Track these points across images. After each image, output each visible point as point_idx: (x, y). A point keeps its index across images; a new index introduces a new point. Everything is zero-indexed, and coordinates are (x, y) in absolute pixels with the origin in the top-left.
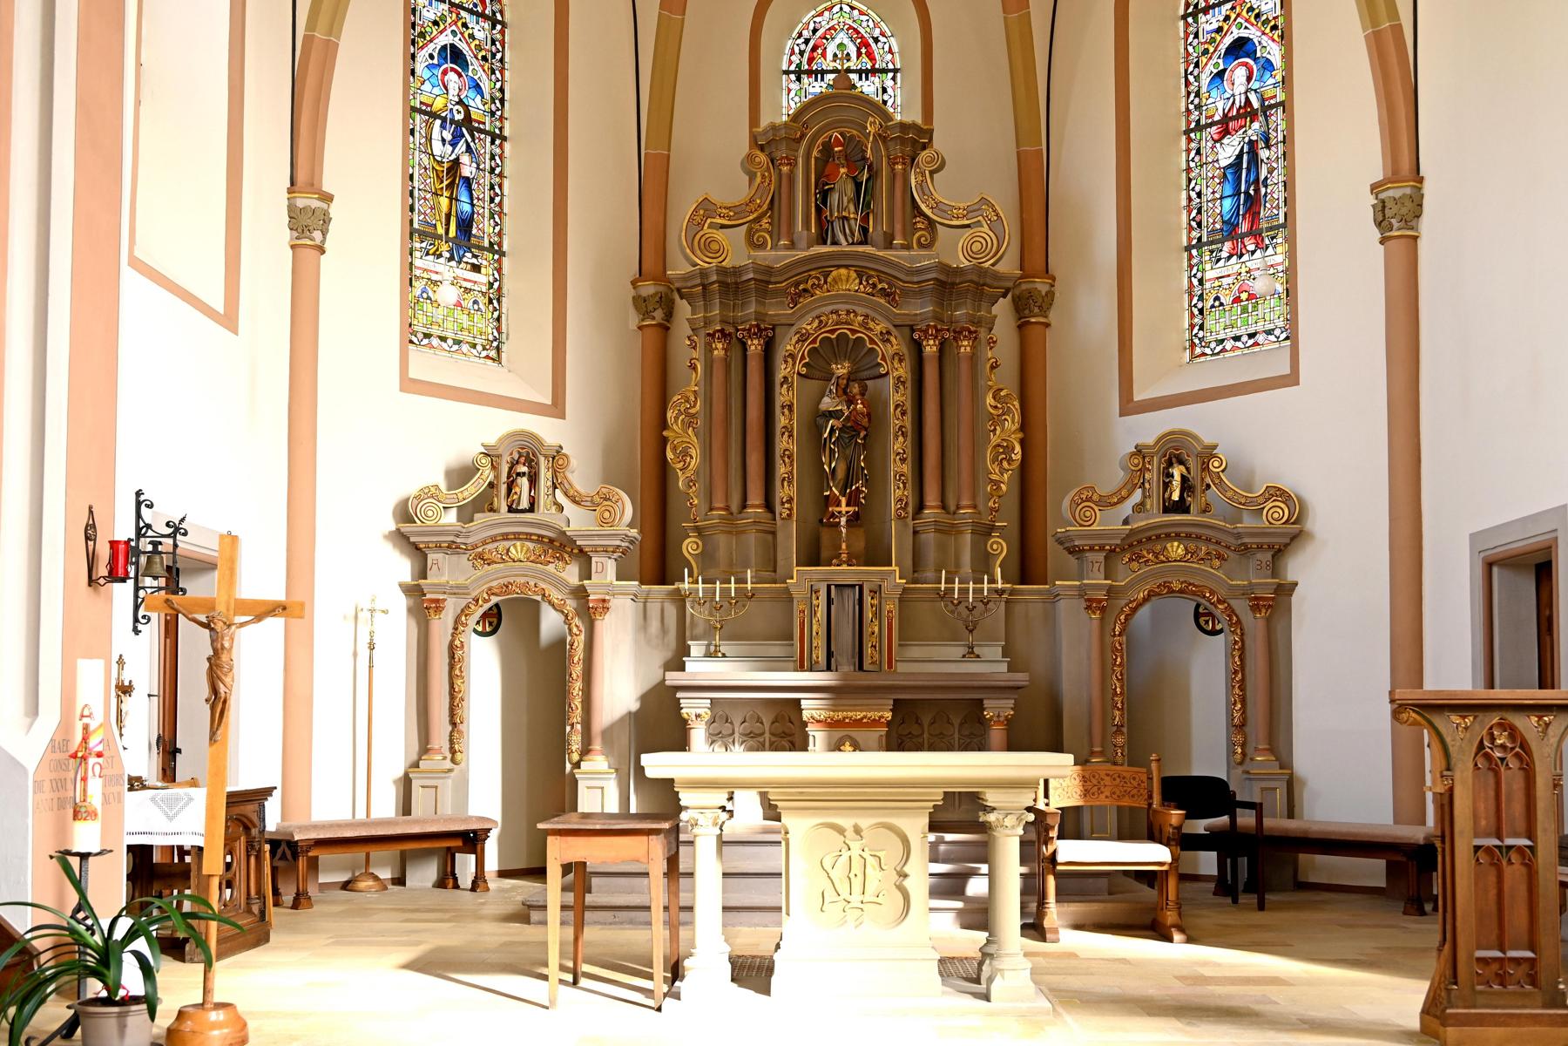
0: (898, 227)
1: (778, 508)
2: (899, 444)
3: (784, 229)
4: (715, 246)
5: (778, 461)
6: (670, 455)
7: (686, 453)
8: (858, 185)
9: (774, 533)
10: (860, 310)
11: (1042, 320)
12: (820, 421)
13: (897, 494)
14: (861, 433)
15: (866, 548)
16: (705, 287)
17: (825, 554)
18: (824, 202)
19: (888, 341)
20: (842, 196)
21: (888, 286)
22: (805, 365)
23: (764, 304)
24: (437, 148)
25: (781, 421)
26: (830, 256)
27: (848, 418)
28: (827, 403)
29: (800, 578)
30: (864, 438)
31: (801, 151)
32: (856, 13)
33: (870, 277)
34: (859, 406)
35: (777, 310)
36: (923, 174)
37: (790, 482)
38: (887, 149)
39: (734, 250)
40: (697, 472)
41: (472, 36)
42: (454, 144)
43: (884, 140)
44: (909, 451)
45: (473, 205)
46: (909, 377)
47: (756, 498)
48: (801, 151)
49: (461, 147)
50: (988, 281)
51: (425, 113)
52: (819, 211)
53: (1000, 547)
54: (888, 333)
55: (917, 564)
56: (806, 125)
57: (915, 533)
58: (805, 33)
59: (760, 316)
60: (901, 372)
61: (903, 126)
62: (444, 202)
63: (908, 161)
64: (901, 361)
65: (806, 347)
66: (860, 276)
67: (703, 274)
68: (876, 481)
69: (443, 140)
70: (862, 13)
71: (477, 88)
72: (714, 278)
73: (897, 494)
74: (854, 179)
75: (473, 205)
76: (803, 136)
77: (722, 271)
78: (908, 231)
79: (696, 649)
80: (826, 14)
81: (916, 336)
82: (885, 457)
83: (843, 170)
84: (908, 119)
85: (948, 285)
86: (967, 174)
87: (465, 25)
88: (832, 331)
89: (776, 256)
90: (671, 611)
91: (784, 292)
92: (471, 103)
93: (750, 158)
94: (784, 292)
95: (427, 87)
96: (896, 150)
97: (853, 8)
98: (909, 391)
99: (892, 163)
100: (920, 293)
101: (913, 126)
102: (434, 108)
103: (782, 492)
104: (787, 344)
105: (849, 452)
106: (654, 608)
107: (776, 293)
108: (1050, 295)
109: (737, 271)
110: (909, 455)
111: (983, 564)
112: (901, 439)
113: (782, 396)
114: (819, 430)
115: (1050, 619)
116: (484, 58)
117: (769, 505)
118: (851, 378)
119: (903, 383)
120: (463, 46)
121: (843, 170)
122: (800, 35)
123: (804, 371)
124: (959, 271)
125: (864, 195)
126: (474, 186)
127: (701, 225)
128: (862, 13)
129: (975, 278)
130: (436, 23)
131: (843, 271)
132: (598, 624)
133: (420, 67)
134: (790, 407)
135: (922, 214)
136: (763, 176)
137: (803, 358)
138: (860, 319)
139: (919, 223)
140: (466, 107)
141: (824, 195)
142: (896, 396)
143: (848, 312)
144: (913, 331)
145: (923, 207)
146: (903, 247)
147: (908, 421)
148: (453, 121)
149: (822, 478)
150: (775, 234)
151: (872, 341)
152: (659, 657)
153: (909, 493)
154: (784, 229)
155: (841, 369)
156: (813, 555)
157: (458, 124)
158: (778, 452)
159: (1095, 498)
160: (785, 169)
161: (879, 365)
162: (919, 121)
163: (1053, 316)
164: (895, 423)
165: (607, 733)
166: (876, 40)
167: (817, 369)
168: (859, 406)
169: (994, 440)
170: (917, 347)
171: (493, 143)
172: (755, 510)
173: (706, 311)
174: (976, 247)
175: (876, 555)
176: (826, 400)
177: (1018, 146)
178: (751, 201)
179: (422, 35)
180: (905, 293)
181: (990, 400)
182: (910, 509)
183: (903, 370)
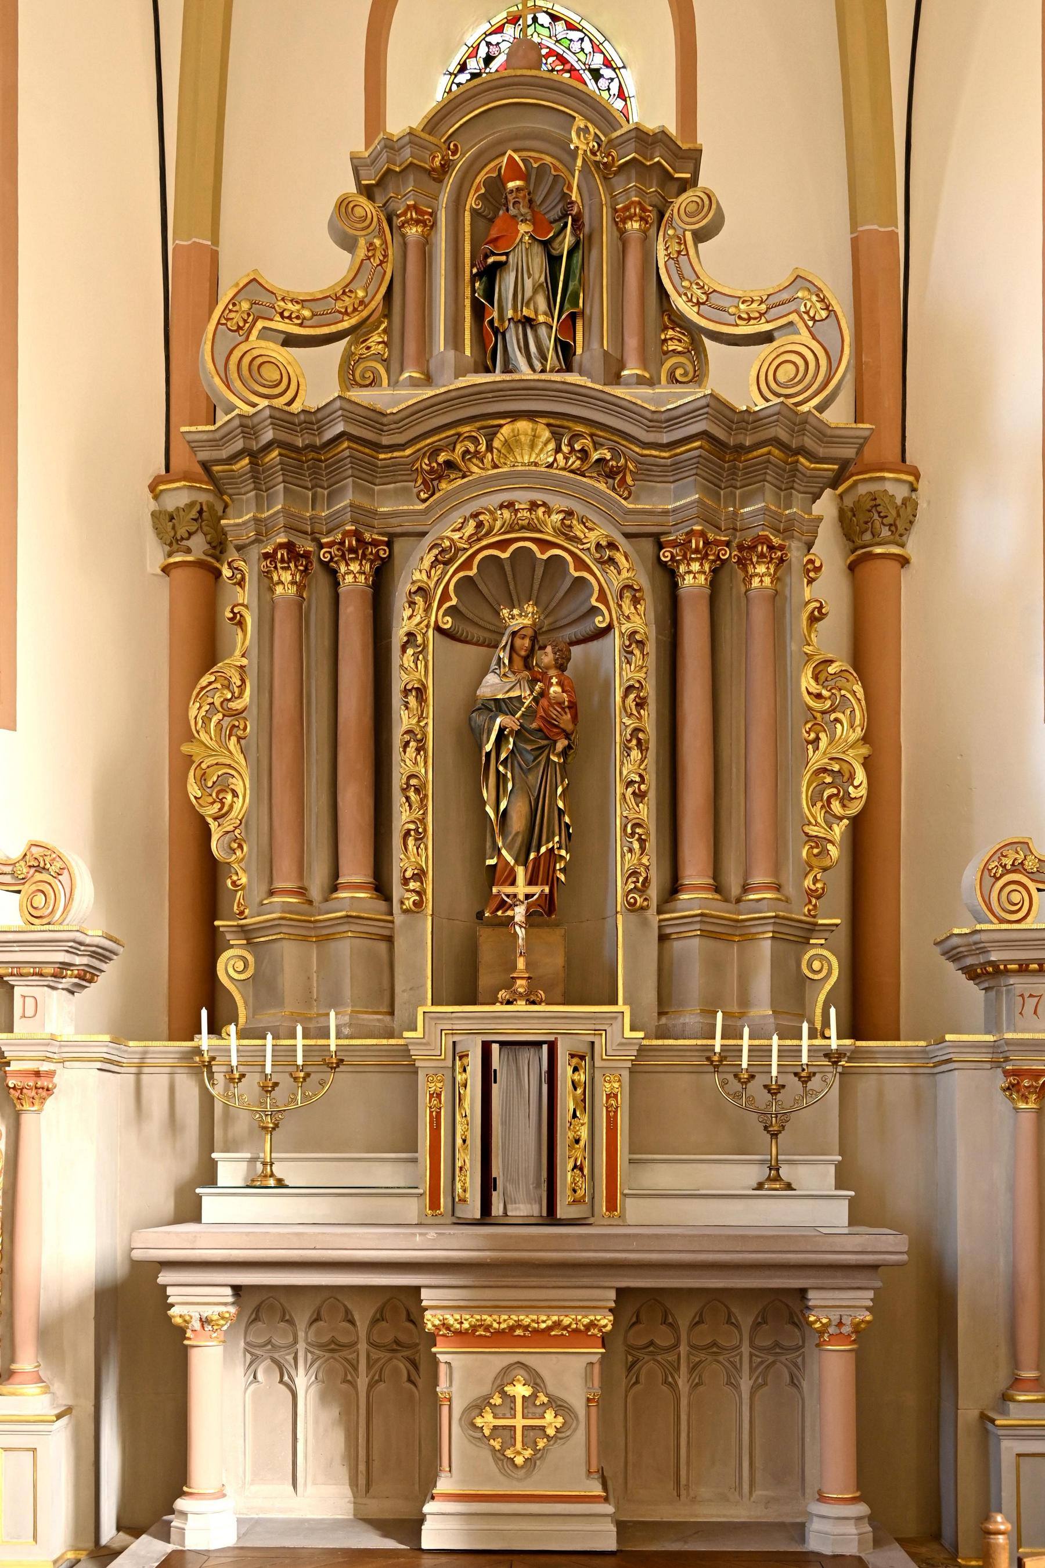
0: (632, 343)
1: (397, 891)
2: (631, 766)
3: (411, 348)
4: (270, 374)
5: (398, 798)
6: (194, 790)
7: (224, 787)
8: (553, 261)
9: (389, 940)
10: (558, 502)
11: (895, 550)
12: (479, 719)
13: (628, 862)
14: (556, 740)
15: (569, 965)
16: (255, 456)
17: (485, 980)
18: (489, 295)
19: (611, 560)
20: (523, 277)
21: (609, 450)
22: (452, 611)
23: (371, 494)
25: (403, 719)
26: (496, 392)
27: (531, 713)
28: (493, 686)
29: (435, 1029)
30: (565, 753)
31: (444, 198)
32: (560, 26)
33: (576, 436)
34: (555, 689)
35: (394, 504)
36: (682, 241)
37: (420, 839)
38: (610, 189)
39: (316, 379)
40: (244, 822)
43: (607, 172)
44: (651, 778)
46: (653, 636)
47: (355, 870)
48: (444, 198)
50: (808, 442)
52: (478, 310)
53: (825, 966)
54: (612, 545)
55: (665, 1002)
56: (452, 146)
57: (663, 938)
58: (473, 65)
59: (362, 515)
60: (637, 623)
61: (642, 138)
63: (652, 216)
64: (636, 601)
65: (452, 576)
66: (557, 437)
67: (247, 427)
68: (586, 833)
70: (570, 27)
72: (268, 435)
73: (628, 862)
74: (546, 245)
76: (446, 167)
77: (282, 419)
78: (653, 354)
79: (231, 1170)
80: (509, 29)
81: (665, 556)
82: (606, 790)
83: (523, 228)
84: (651, 125)
85: (729, 449)
86: (764, 228)
88: (502, 545)
89: (393, 396)
90: (188, 1089)
91: (410, 470)
93: (344, 206)
94: (410, 470)
96: (628, 188)
97: (555, 18)
98: (651, 661)
99: (620, 219)
100: (673, 471)
101: (661, 138)
103: (405, 859)
104: (416, 569)
105: (534, 779)
106: (156, 1085)
107: (392, 472)
108: (910, 505)
109: (313, 420)
110: (651, 785)
111: (792, 993)
112: (635, 754)
113: (405, 670)
114: (476, 737)
115: (925, 1108)
118: (537, 639)
119: (641, 644)
121: (523, 228)
122: (463, 68)
123: (447, 623)
124: (749, 420)
125: (564, 277)
127: (243, 330)
128: (570, 27)
129: (783, 435)
131: (523, 425)
132: (27, 1119)
134: (420, 692)
135: (678, 321)
136: (371, 246)
137: (445, 597)
138: (556, 518)
139: (677, 335)
141: (489, 274)
142: (625, 669)
143: (534, 506)
144: (660, 546)
145: (679, 303)
146: (640, 381)
147: (649, 719)
149: (482, 831)
150: (393, 363)
151: (581, 564)
152: (161, 1176)
153: (650, 861)
154: (411, 348)
155: (520, 618)
156: (463, 984)
159: (1030, 864)
160: (413, 232)
161: (594, 611)
162: (672, 129)
163: (913, 548)
164: (623, 724)
165: (48, 1336)
166: (596, 74)
167: (470, 623)
168: (555, 689)
169: (816, 759)
170: (669, 576)
172: (356, 896)
173: (259, 508)
174: (786, 373)
175: (585, 982)
176: (491, 679)
177: (854, 223)
178: (346, 290)
180: (646, 471)
181: (807, 682)
182: (653, 892)
183: (639, 620)
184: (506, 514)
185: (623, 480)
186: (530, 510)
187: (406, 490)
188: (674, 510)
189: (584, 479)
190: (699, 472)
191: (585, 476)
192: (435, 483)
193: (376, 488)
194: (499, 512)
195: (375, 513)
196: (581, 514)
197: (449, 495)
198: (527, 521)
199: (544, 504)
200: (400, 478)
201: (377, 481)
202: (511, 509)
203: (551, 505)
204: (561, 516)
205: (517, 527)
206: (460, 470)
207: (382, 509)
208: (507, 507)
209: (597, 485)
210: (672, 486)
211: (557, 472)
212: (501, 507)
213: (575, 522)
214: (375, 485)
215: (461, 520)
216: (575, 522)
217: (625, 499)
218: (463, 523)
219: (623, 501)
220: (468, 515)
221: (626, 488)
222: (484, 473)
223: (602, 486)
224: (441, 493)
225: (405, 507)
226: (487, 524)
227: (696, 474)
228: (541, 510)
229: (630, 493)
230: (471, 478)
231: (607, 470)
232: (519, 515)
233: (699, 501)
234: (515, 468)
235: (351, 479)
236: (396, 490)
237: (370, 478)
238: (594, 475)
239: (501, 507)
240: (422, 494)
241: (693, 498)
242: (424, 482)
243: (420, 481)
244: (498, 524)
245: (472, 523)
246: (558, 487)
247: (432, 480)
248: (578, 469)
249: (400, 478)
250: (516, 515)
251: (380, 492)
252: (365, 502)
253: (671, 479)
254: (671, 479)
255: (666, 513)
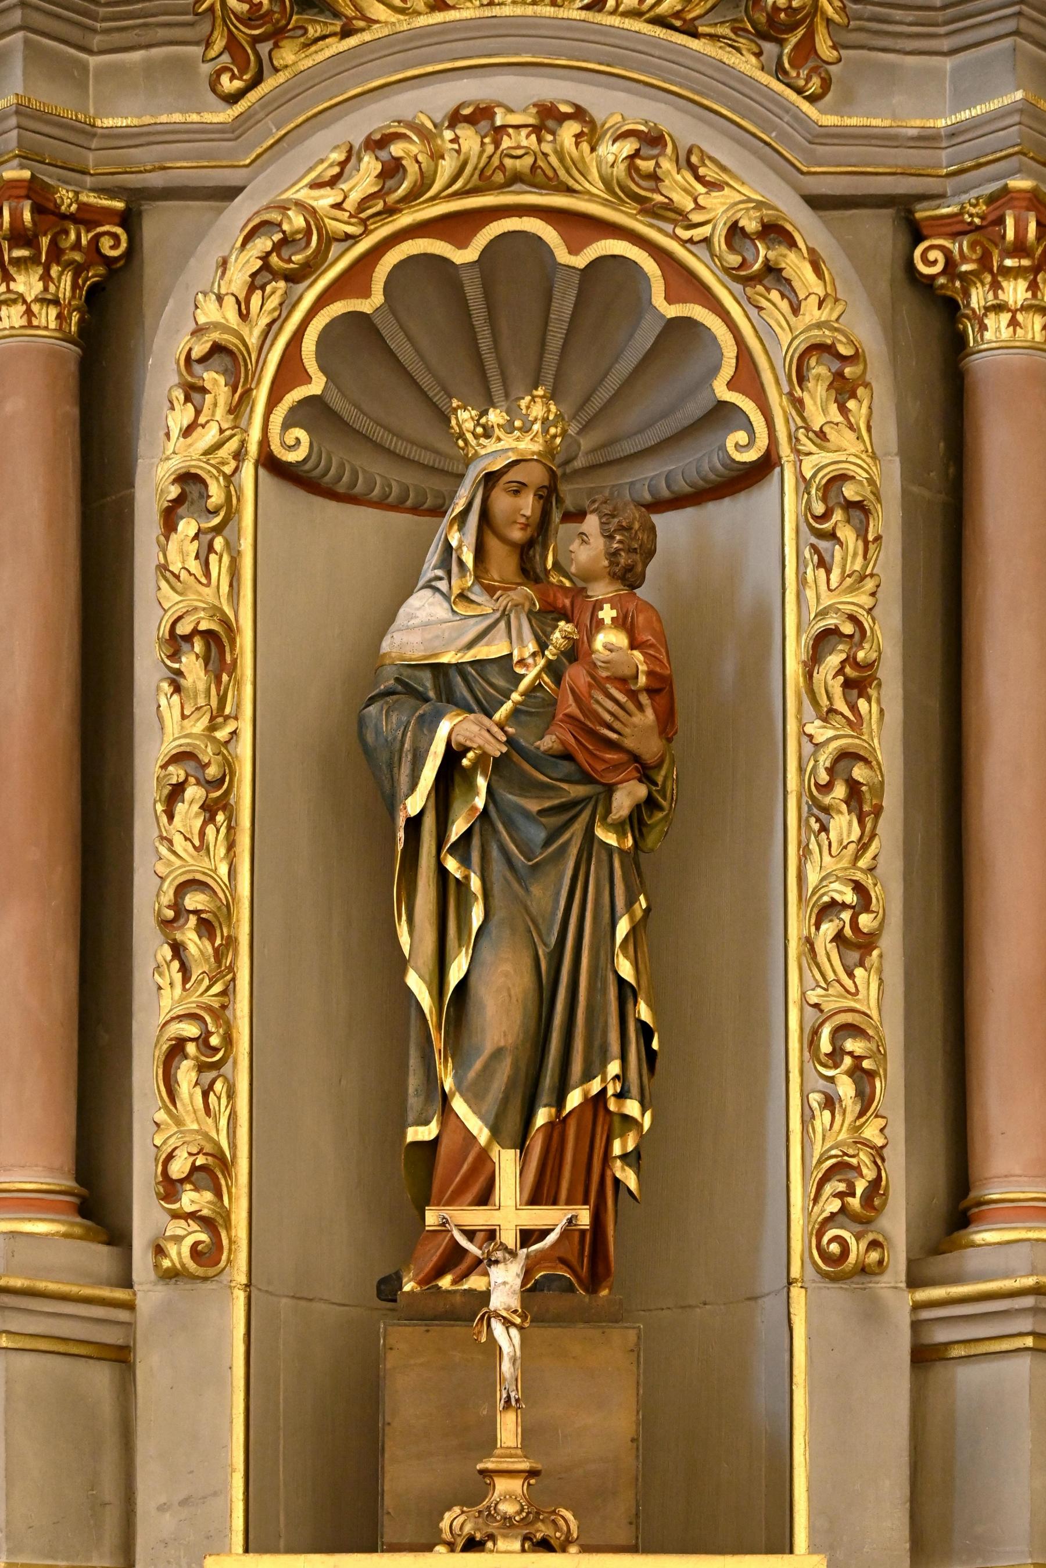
1: (146, 1216)
2: (830, 865)
5: (149, 949)
9: (121, 1357)
10: (613, 107)
12: (388, 722)
13: (821, 1130)
14: (612, 788)
15: (647, 1439)
17: (403, 1477)
19: (772, 272)
22: (313, 413)
23: (76, 77)
25: (165, 722)
27: (538, 707)
28: (429, 626)
30: (637, 821)
34: (608, 641)
37: (213, 1064)
44: (889, 893)
46: (892, 484)
54: (774, 231)
57: (925, 1356)
60: (846, 451)
64: (843, 389)
65: (311, 313)
73: (821, 1130)
81: (929, 261)
82: (757, 926)
88: (456, 226)
98: (889, 561)
103: (165, 1125)
104: (205, 292)
105: (547, 895)
110: (889, 915)
112: (844, 825)
113: (171, 580)
114: (377, 773)
117: (96, 1200)
118: (556, 498)
123: (296, 446)
134: (216, 644)
137: (291, 370)
138: (614, 152)
142: (806, 577)
143: (548, 117)
144: (916, 234)
147: (884, 727)
149: (397, 1044)
151: (684, 282)
153: (890, 1134)
155: (509, 435)
158: (149, 894)
161: (722, 415)
164: (807, 737)
168: (608, 641)
176: (424, 608)
182: (896, 1224)
183: (856, 442)
184: (470, 139)
185: (807, 48)
186: (537, 130)
187: (183, 68)
188: (953, 133)
189: (695, 44)
190: (1025, 26)
191: (695, 35)
192: (264, 48)
193: (93, 61)
194: (448, 135)
195: (89, 131)
196: (686, 140)
197: (304, 84)
198: (529, 160)
199: (579, 113)
200: (162, 33)
201: (96, 41)
202: (484, 125)
203: (598, 116)
204: (628, 147)
205: (499, 177)
206: (337, 15)
207: (109, 122)
208: (471, 120)
209: (731, 58)
210: (948, 63)
211: (616, 21)
212: (455, 119)
213: (667, 165)
214: (90, 52)
215: (338, 156)
216: (667, 165)
217: (812, 99)
218: (343, 164)
219: (805, 106)
220: (358, 141)
221: (814, 70)
222: (404, 23)
223: (746, 64)
224: (281, 77)
225: (177, 117)
226: (412, 169)
227: (1016, 33)
228: (569, 130)
229: (826, 84)
230: (366, 36)
231: (762, 18)
232: (506, 143)
233: (1027, 109)
234: (496, 11)
235: (20, 35)
236: (149, 68)
237: (75, 34)
238: (724, 30)
239: (455, 119)
240: (225, 79)
241: (1007, 100)
242: (232, 45)
243: (219, 44)
244: (447, 167)
245: (370, 165)
246: (615, 64)
247: (255, 40)
248: (677, 15)
249: (162, 33)
250: (497, 144)
251: (103, 72)
252: (56, 99)
253: (946, 44)
254: (946, 44)
255: (928, 139)
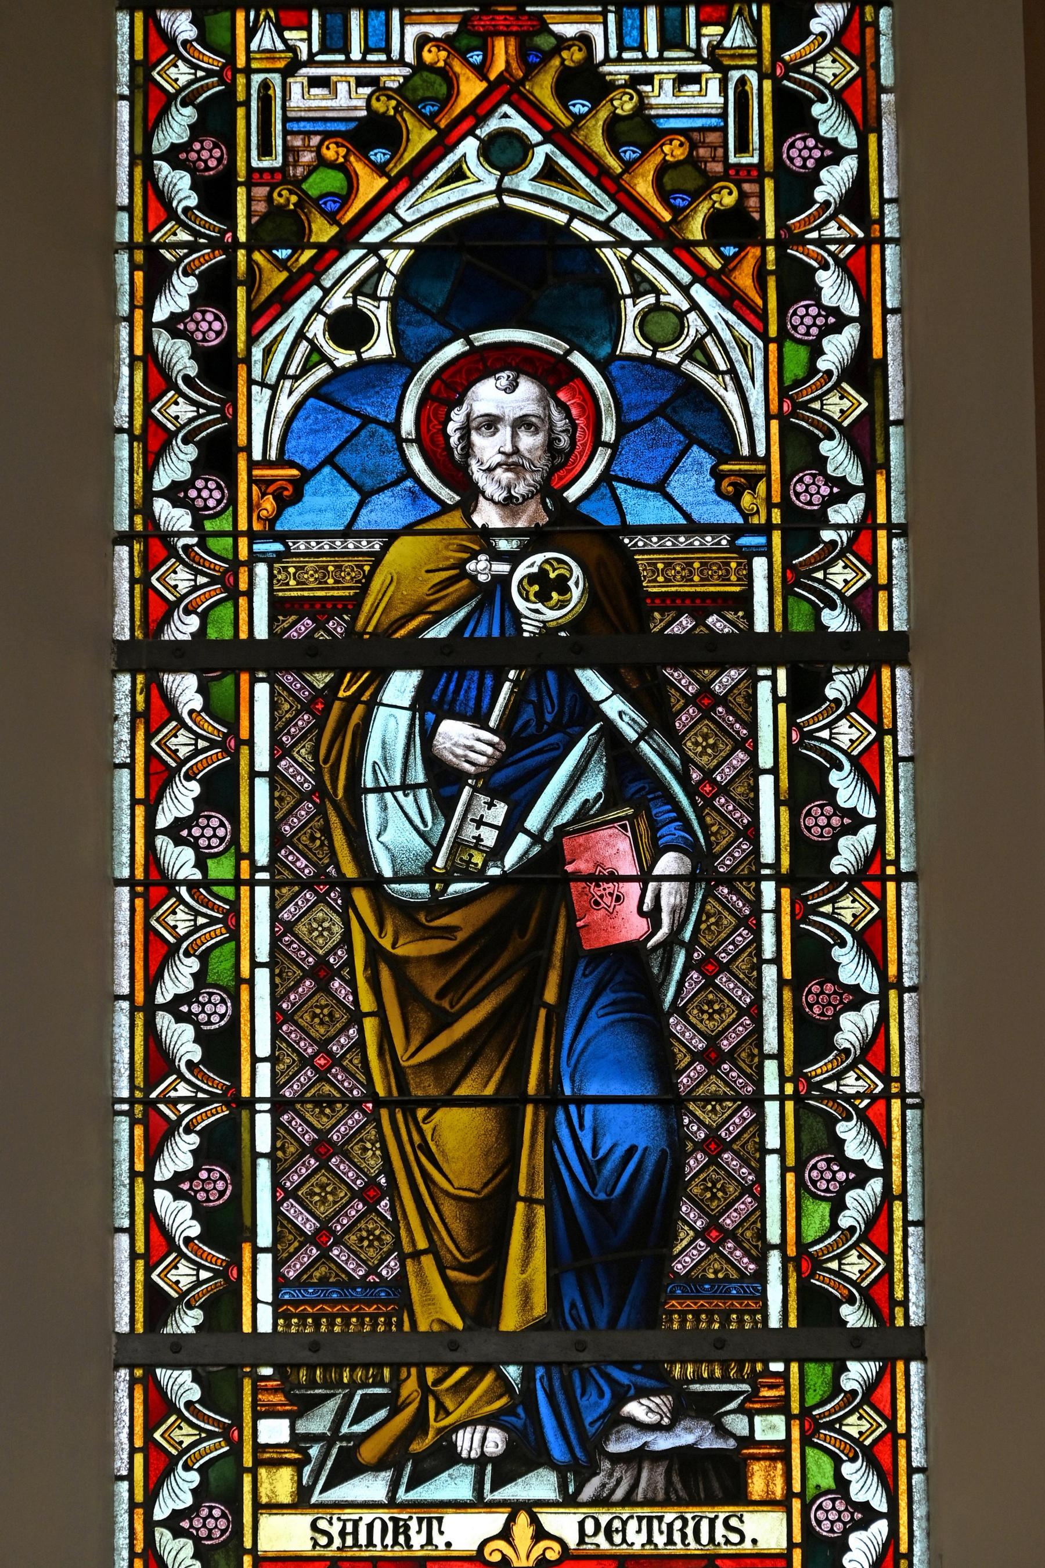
24: (394, 832)
41: (640, 130)
42: (514, 780)
45: (670, 1103)
49: (574, 782)
51: (307, 656)
62: (459, 1134)
69: (444, 781)
71: (684, 411)
75: (670, 1103)
87: (585, 81)
92: (644, 509)
95: (325, 505)
102: (371, 617)
116: (733, 228)
120: (579, 209)
126: (677, 980)
130: (372, 133)
133: (263, 418)
140: (606, 549)
148: (510, 648)
157: (550, 660)
171: (804, 696)
179: (280, 227)
